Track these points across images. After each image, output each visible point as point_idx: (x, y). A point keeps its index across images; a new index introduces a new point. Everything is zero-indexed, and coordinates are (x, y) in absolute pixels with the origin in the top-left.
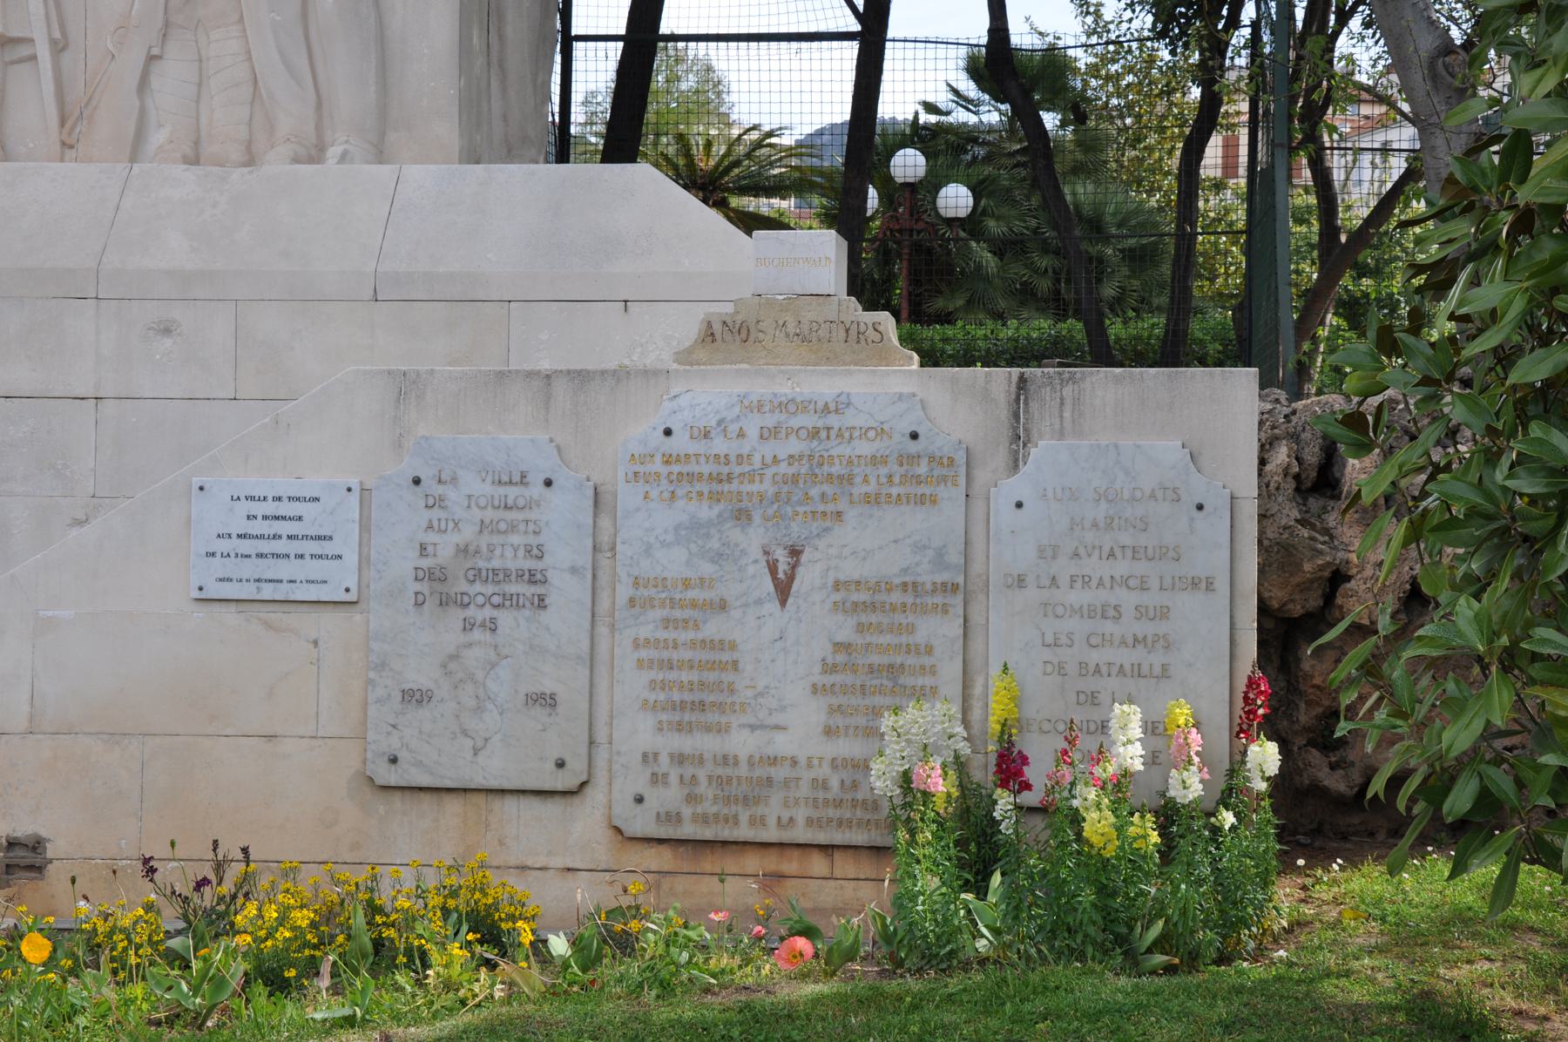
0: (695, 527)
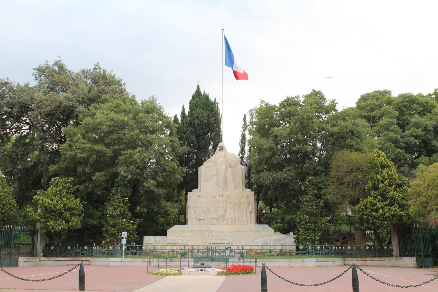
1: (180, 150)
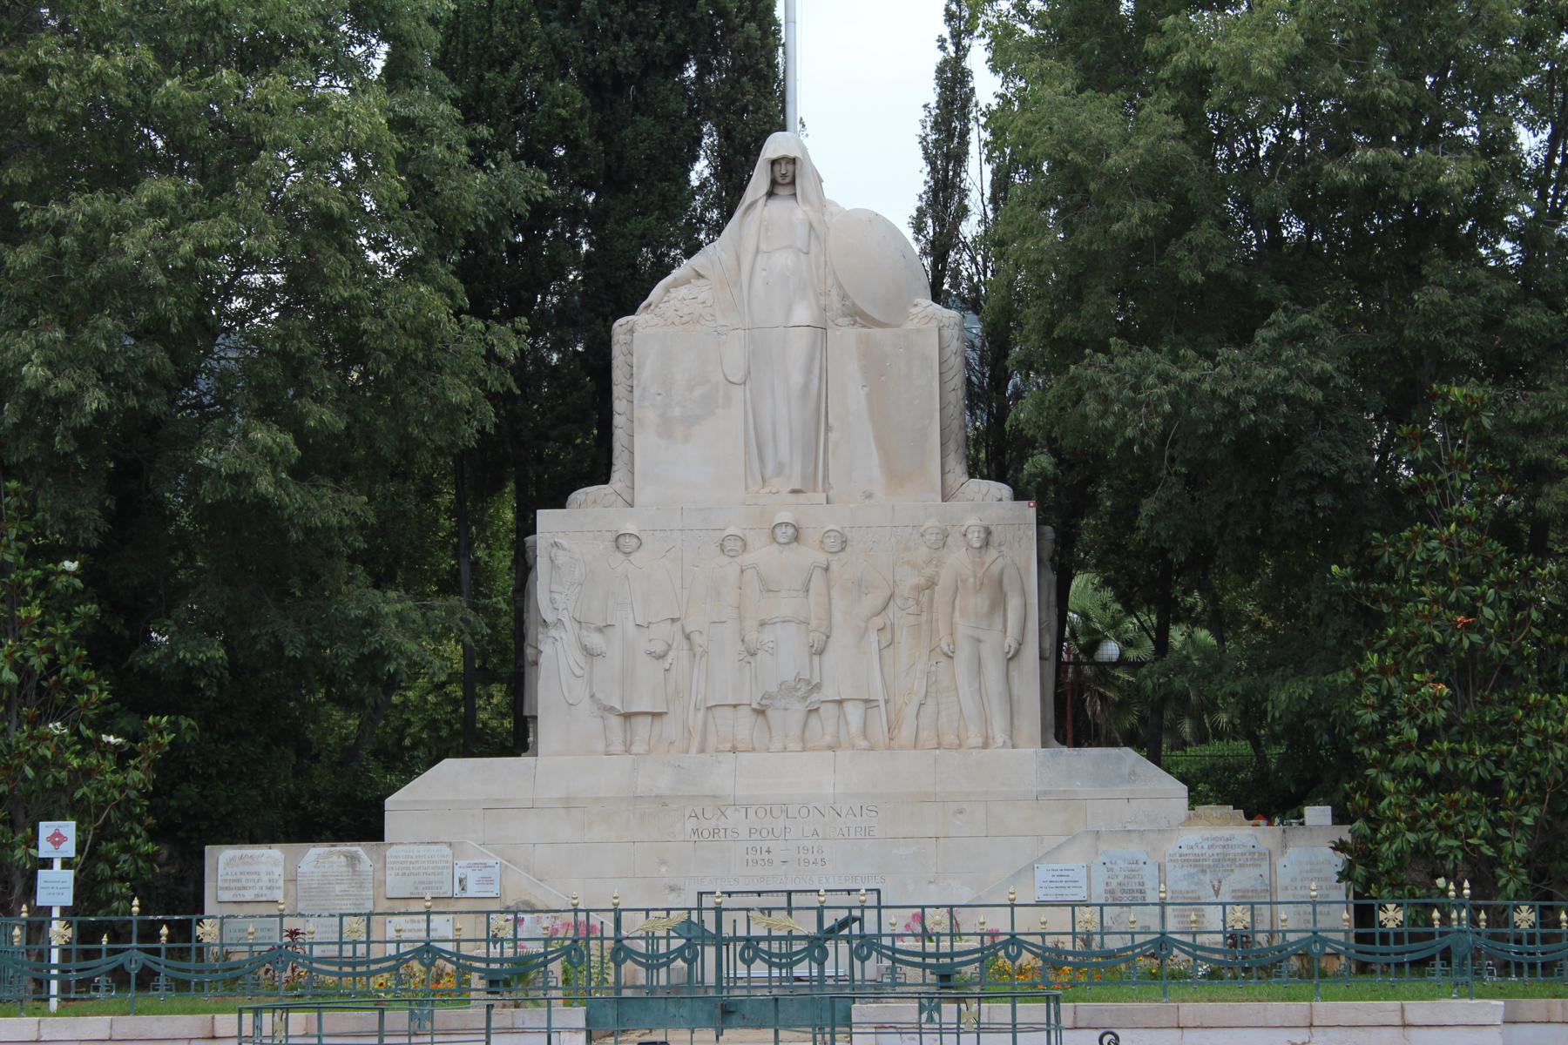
0: (1190, 875)
1: (472, 190)
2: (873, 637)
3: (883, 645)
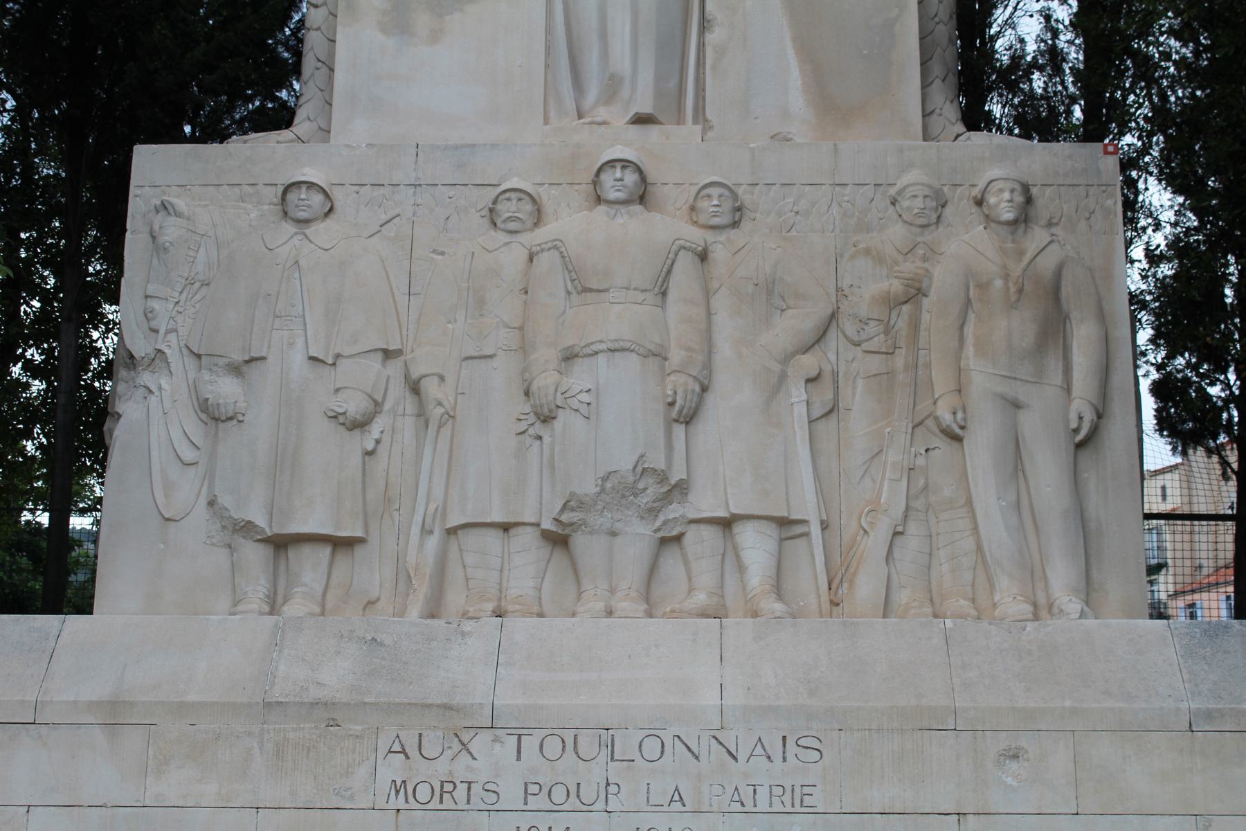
2: (797, 393)
3: (817, 413)
